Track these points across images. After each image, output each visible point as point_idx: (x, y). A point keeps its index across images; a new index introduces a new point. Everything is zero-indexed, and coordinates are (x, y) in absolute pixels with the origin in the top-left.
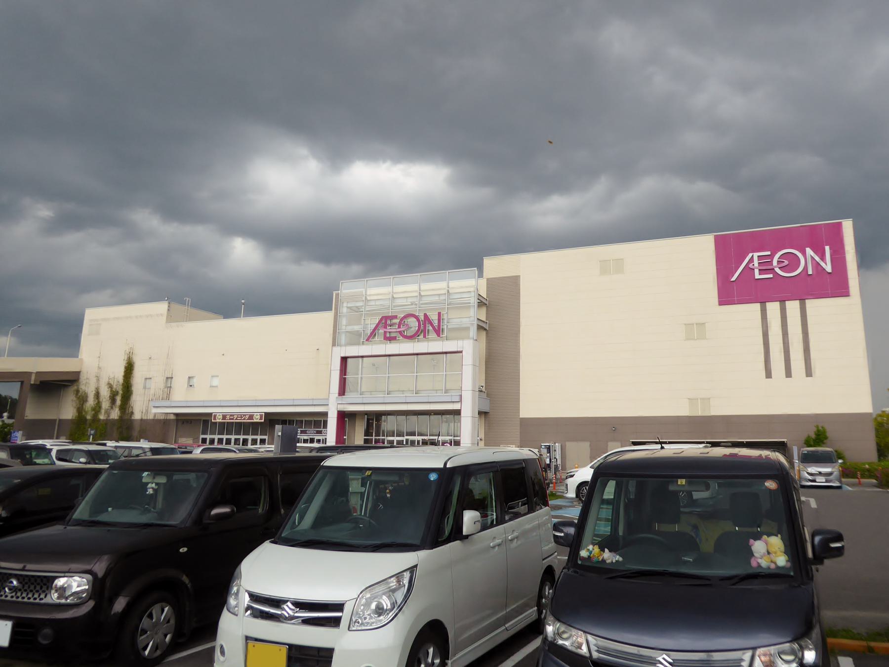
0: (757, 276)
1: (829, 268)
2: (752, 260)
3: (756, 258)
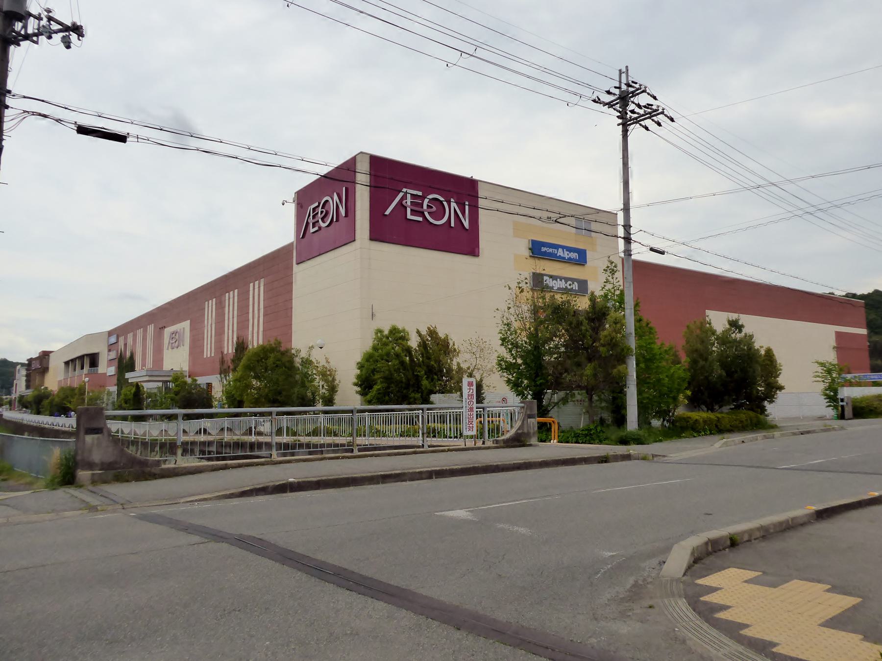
0: (409, 216)
2: (404, 197)
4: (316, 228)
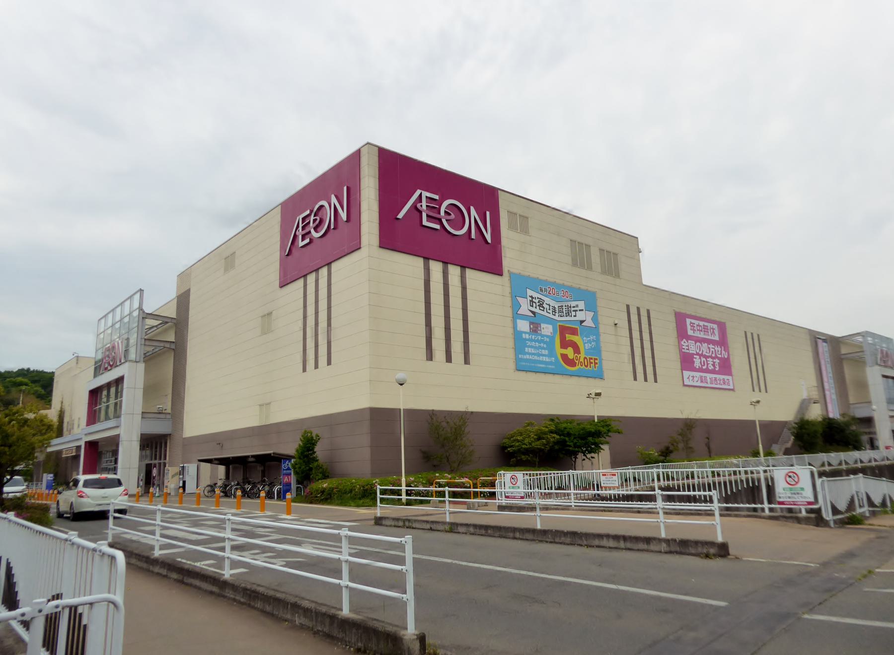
3: (424, 199)
4: (307, 241)
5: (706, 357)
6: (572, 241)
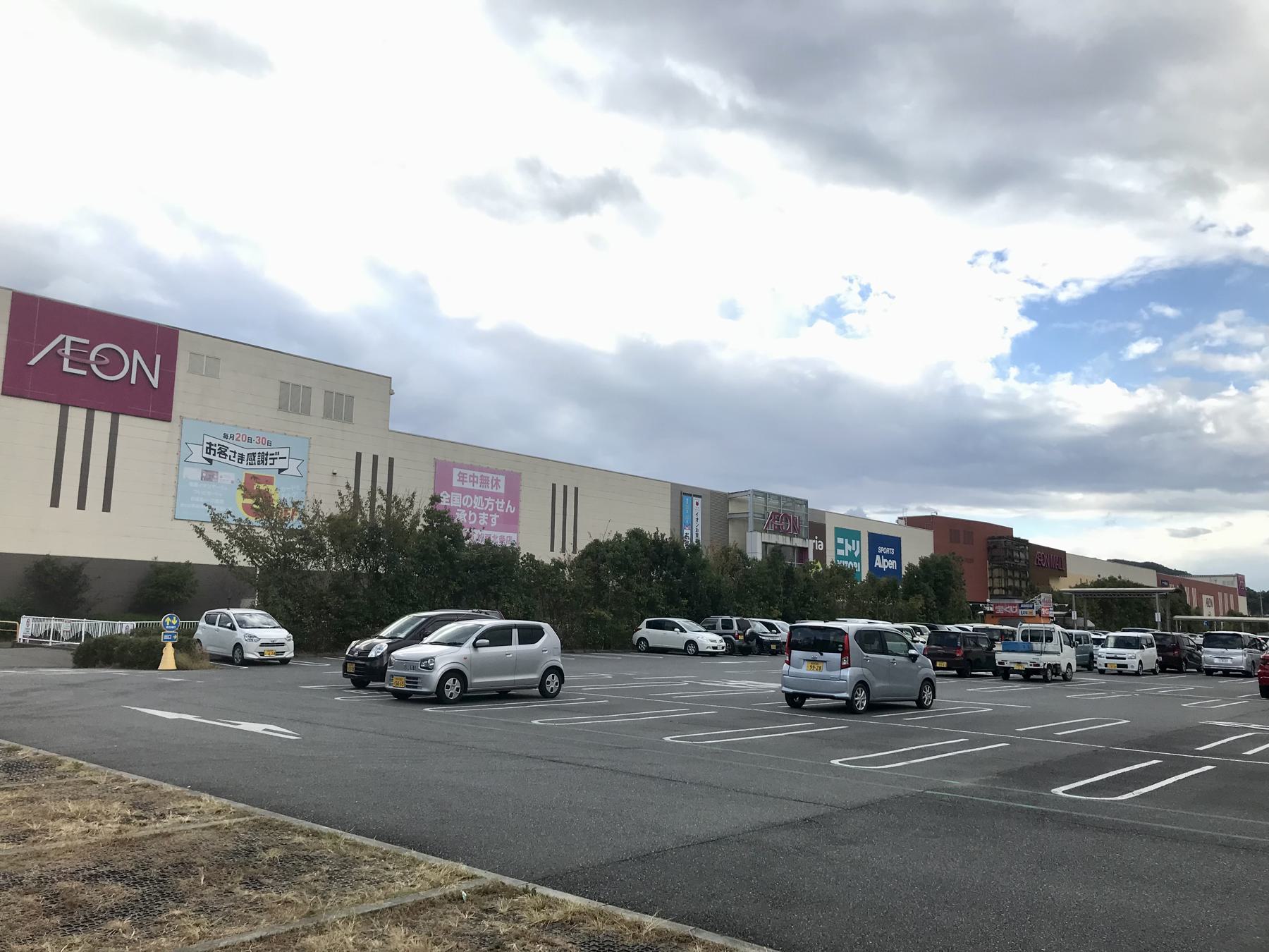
0: (66, 368)
1: (155, 385)
3: (68, 344)
5: (478, 512)
6: (284, 384)
